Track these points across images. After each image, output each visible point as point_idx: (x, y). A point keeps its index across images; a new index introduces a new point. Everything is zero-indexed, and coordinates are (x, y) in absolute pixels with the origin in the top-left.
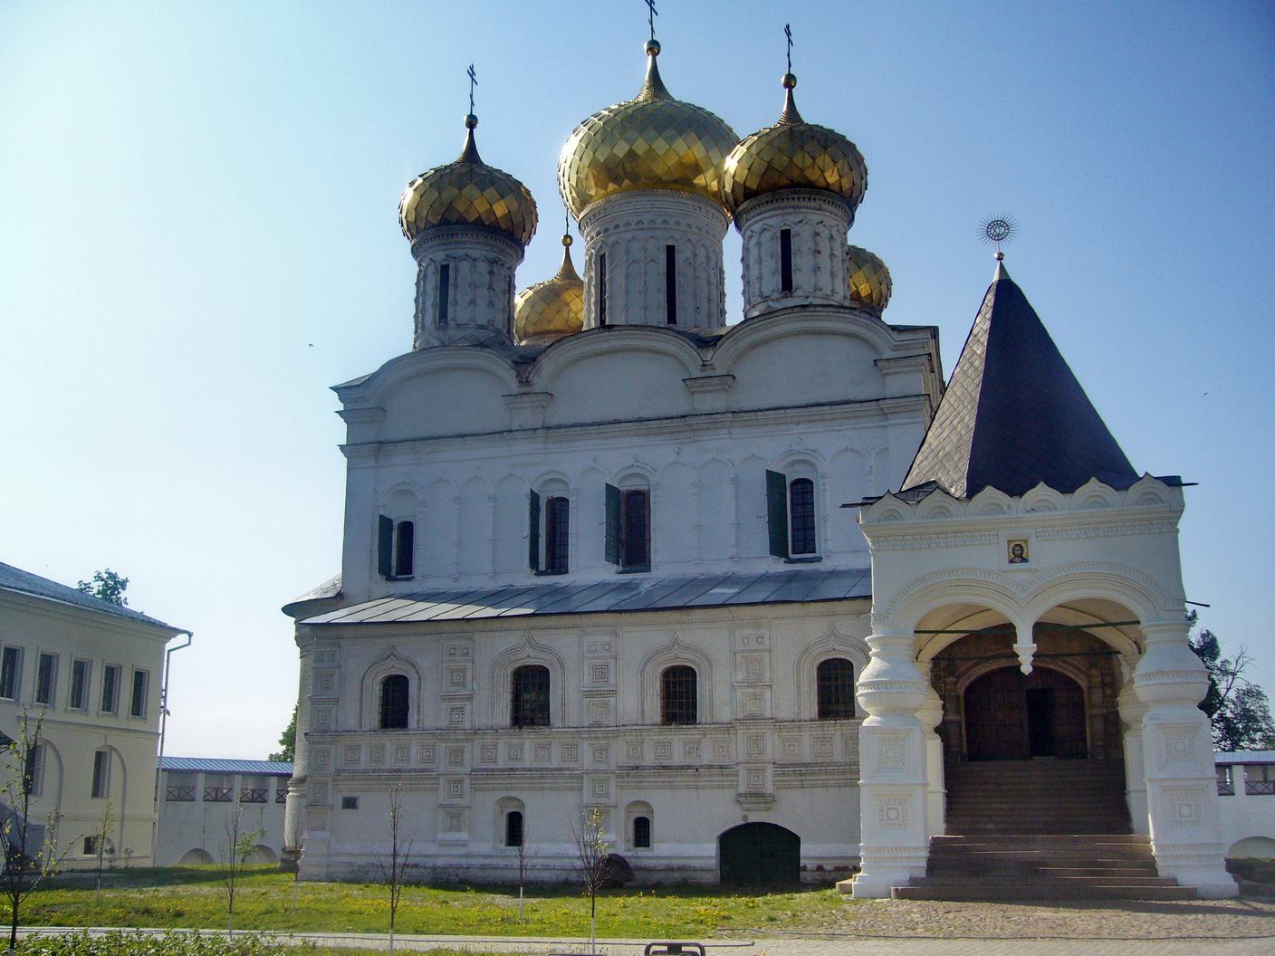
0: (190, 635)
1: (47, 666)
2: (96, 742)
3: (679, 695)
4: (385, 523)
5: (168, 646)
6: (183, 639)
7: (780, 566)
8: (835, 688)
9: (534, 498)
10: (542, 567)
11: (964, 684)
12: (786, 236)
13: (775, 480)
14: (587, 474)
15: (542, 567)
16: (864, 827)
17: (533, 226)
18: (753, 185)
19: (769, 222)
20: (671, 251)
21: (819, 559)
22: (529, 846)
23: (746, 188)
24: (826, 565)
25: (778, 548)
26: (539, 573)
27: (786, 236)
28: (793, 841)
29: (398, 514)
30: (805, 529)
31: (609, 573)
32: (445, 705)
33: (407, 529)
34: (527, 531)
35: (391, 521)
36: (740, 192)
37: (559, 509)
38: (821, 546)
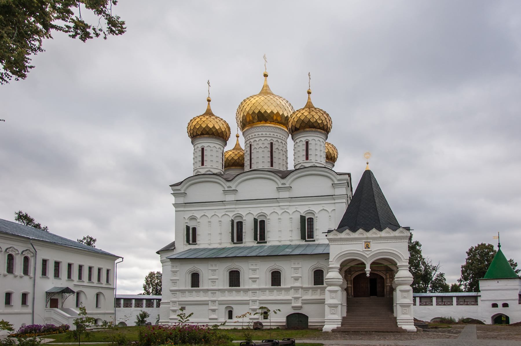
0: (123, 258)
1: (57, 264)
2: (97, 291)
3: (276, 278)
4: (188, 228)
5: (116, 262)
6: (120, 259)
7: (303, 243)
8: (319, 277)
9: (232, 221)
10: (235, 241)
11: (353, 276)
12: (307, 143)
13: (303, 218)
14: (248, 215)
15: (235, 241)
16: (326, 313)
17: (229, 135)
18: (298, 126)
19: (301, 139)
21: (314, 241)
22: (235, 319)
23: (295, 127)
24: (316, 242)
25: (303, 238)
26: (234, 243)
27: (307, 143)
28: (307, 317)
29: (192, 225)
30: (311, 232)
31: (255, 244)
32: (210, 281)
33: (194, 229)
34: (231, 231)
35: (189, 227)
36: (294, 128)
37: (240, 225)
38: (315, 237)
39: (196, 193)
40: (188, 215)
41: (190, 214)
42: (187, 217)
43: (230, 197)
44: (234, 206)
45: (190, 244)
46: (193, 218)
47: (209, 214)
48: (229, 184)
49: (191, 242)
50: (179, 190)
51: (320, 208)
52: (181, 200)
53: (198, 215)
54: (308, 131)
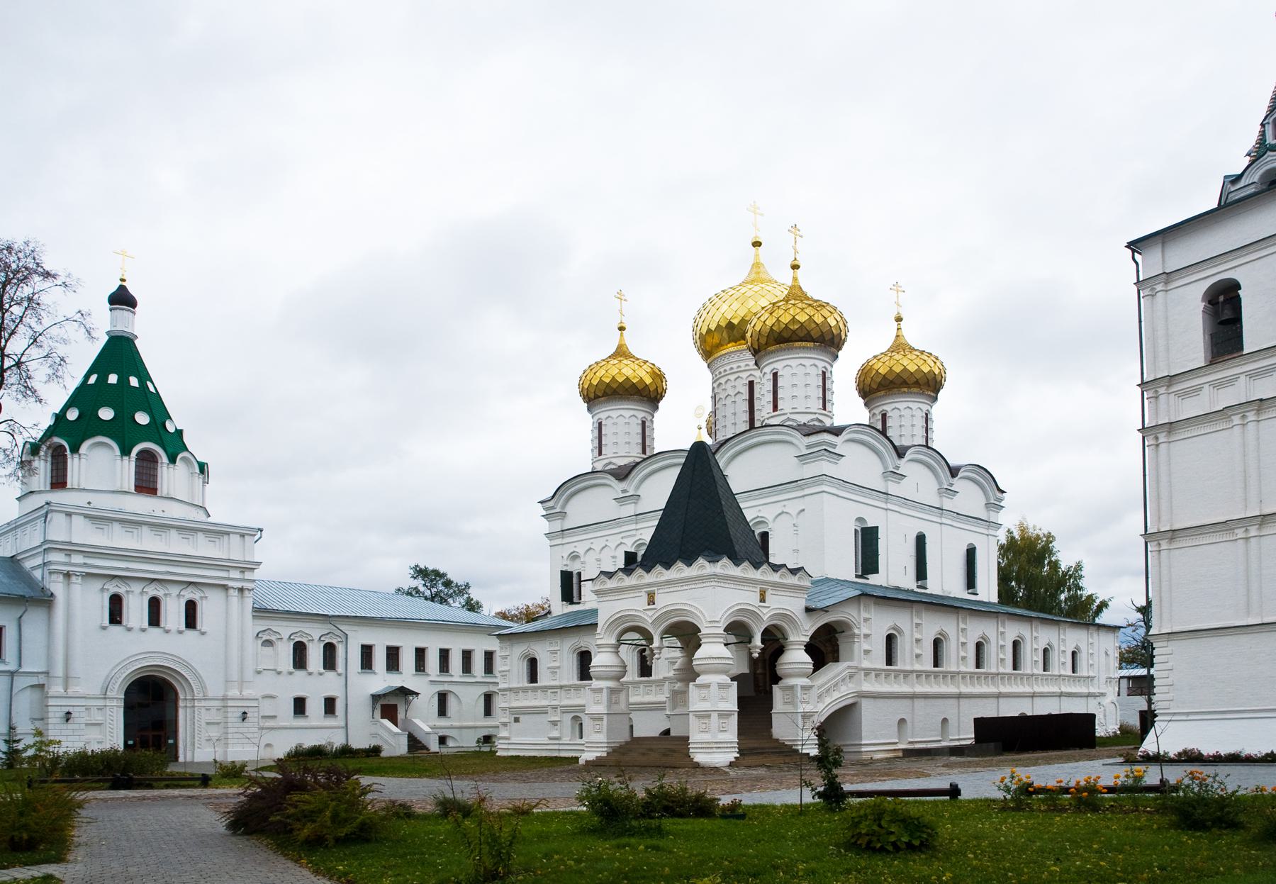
20: (751, 384)
39: (583, 509)
40: (569, 549)
41: (570, 549)
42: (566, 556)
43: (629, 510)
44: (633, 526)
45: (572, 603)
46: (574, 557)
47: (597, 545)
48: (623, 485)
49: (575, 600)
50: (553, 508)
51: (778, 508)
52: (557, 525)
53: (581, 549)
54: (772, 352)
